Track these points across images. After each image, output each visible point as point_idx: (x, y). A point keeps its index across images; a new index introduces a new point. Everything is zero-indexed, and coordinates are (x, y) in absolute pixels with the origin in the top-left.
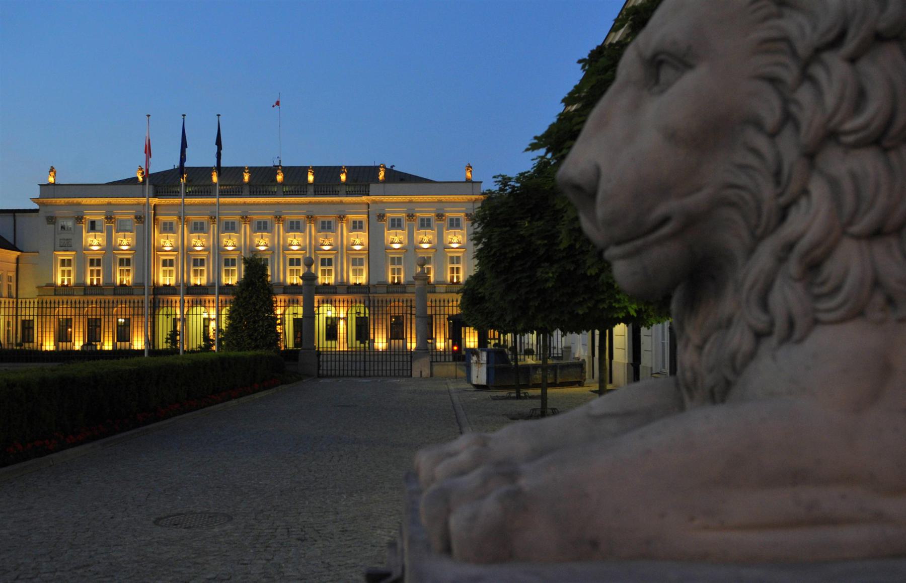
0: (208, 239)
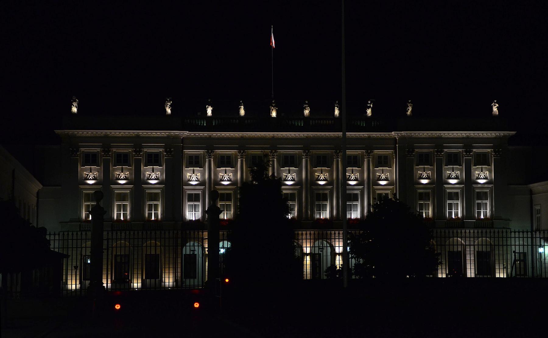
0: (235, 173)
